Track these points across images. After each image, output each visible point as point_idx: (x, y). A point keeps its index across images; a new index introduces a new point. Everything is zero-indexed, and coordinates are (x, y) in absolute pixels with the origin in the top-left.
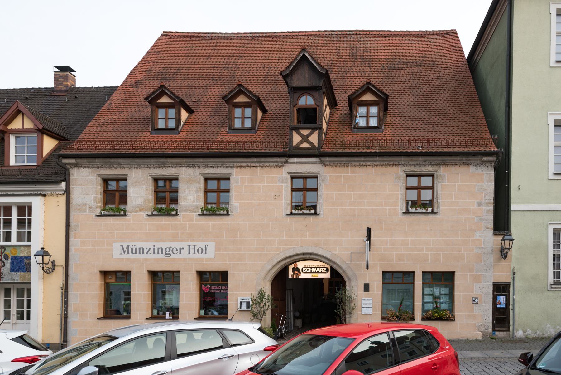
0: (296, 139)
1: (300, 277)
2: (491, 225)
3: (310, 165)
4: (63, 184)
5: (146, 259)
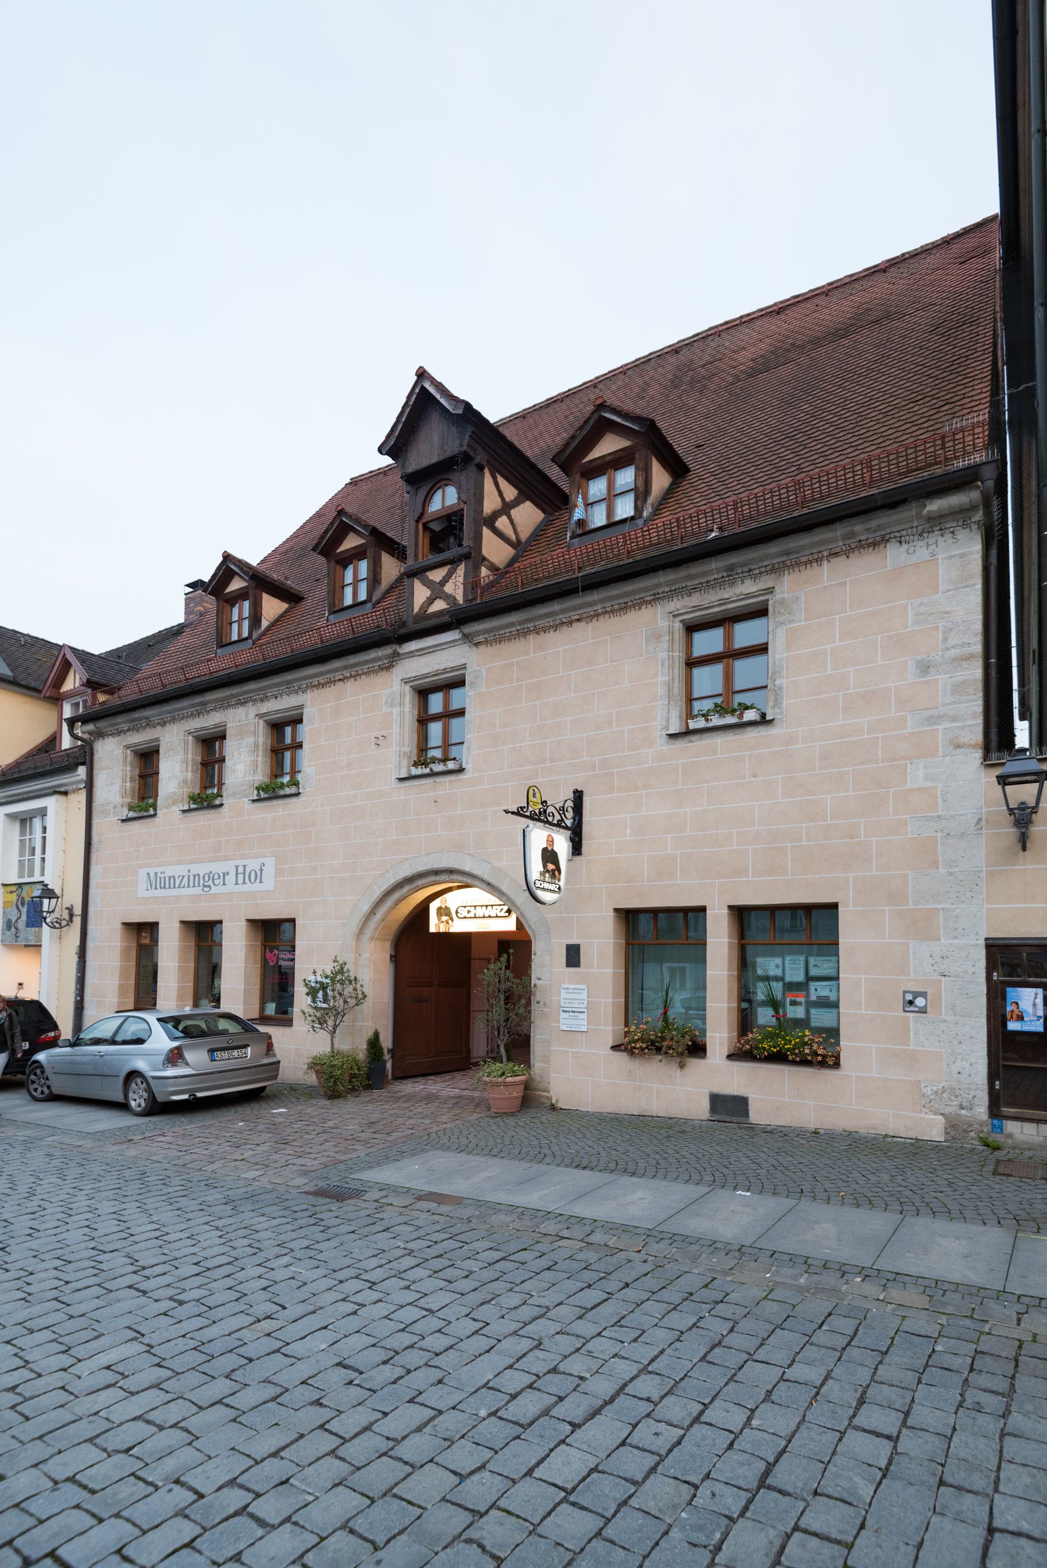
0: (421, 593)
1: (452, 930)
2: (978, 737)
3: (446, 652)
4: (82, 771)
5: (178, 898)
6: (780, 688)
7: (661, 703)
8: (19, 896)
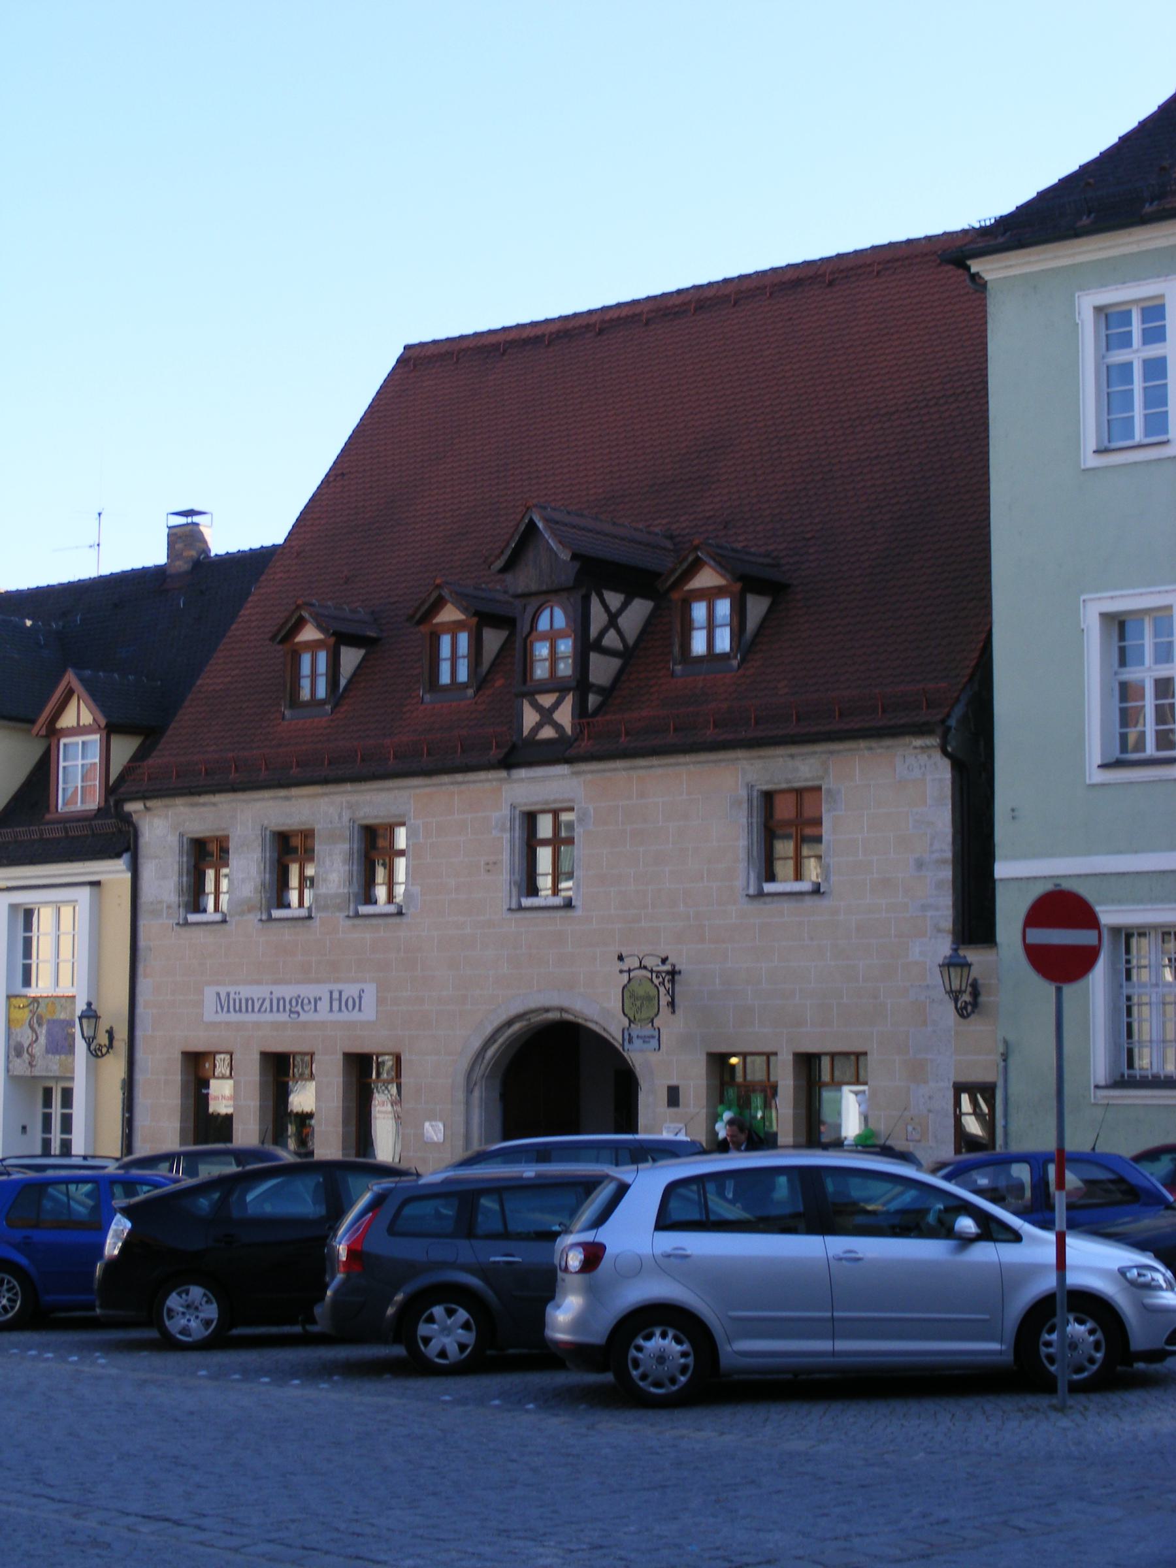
2: (948, 924)
5: (257, 1025)
6: (829, 866)
7: (742, 865)
8: (33, 1013)
